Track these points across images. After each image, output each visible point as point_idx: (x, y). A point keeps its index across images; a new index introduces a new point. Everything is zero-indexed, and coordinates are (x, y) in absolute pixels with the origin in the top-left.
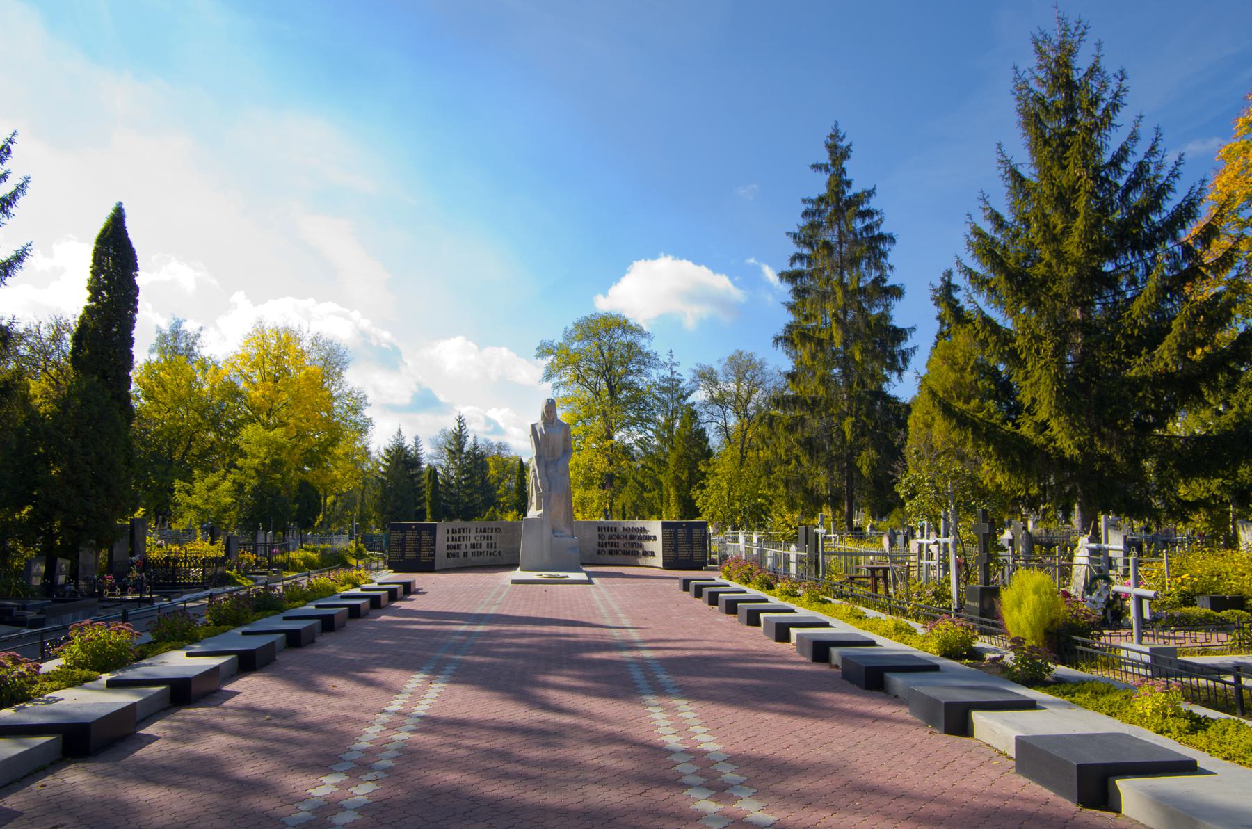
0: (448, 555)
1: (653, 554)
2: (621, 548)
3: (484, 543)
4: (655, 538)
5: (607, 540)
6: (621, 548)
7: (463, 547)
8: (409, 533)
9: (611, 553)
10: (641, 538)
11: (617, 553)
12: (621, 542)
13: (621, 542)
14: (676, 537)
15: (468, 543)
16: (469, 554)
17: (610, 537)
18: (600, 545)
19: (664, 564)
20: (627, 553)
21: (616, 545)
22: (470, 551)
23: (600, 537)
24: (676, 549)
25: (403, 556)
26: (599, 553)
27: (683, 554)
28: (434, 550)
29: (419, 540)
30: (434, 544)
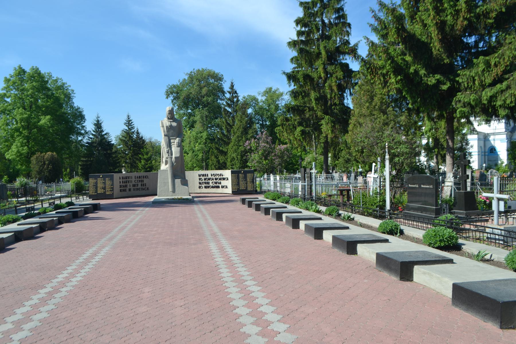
0: (121, 191)
2: (211, 184)
3: (140, 184)
5: (203, 181)
6: (211, 184)
7: (128, 186)
9: (206, 187)
11: (208, 187)
12: (211, 182)
13: (211, 182)
14: (238, 178)
15: (131, 184)
16: (132, 190)
17: (205, 179)
18: (200, 183)
19: (232, 191)
20: (213, 187)
21: (208, 183)
22: (132, 188)
23: (200, 179)
24: (238, 184)
25: (96, 191)
26: (200, 187)
27: (242, 187)
28: (113, 188)
29: (105, 183)
30: (113, 185)
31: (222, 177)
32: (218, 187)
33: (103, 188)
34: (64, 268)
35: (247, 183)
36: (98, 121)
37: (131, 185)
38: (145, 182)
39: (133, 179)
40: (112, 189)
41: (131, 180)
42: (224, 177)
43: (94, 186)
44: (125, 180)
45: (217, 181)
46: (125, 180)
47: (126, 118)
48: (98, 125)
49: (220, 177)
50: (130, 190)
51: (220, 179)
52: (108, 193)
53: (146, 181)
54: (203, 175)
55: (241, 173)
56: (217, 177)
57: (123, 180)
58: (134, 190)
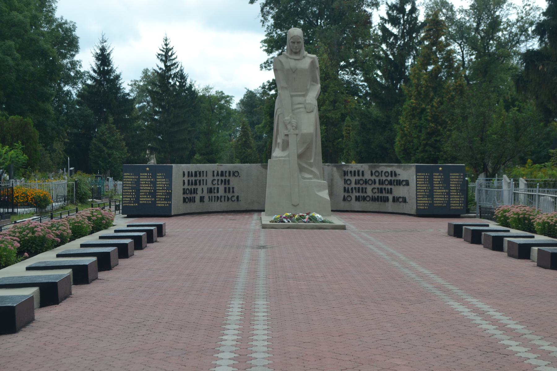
0: (184, 200)
1: (405, 200)
2: (369, 193)
3: (222, 188)
4: (407, 183)
5: (353, 185)
6: (369, 193)
7: (199, 191)
8: (143, 176)
9: (358, 199)
11: (364, 199)
12: (369, 188)
16: (206, 199)
20: (374, 199)
21: (364, 190)
23: (346, 181)
24: (431, 195)
25: (137, 200)
26: (344, 199)
28: (170, 194)
29: (154, 183)
30: (170, 187)
31: (394, 178)
32: (386, 200)
33: (150, 193)
34: (218, 326)
35: (448, 194)
36: (103, 49)
37: (205, 191)
38: (231, 185)
39: (210, 178)
40: (169, 196)
41: (205, 178)
42: (398, 178)
43: (132, 188)
44: (193, 179)
45: (384, 186)
46: (193, 179)
47: (161, 45)
48: (103, 58)
49: (389, 178)
50: (202, 199)
51: (390, 183)
52: (160, 204)
53: (234, 182)
54: (354, 173)
55: (438, 171)
56: (384, 178)
57: (190, 179)
58: (210, 199)
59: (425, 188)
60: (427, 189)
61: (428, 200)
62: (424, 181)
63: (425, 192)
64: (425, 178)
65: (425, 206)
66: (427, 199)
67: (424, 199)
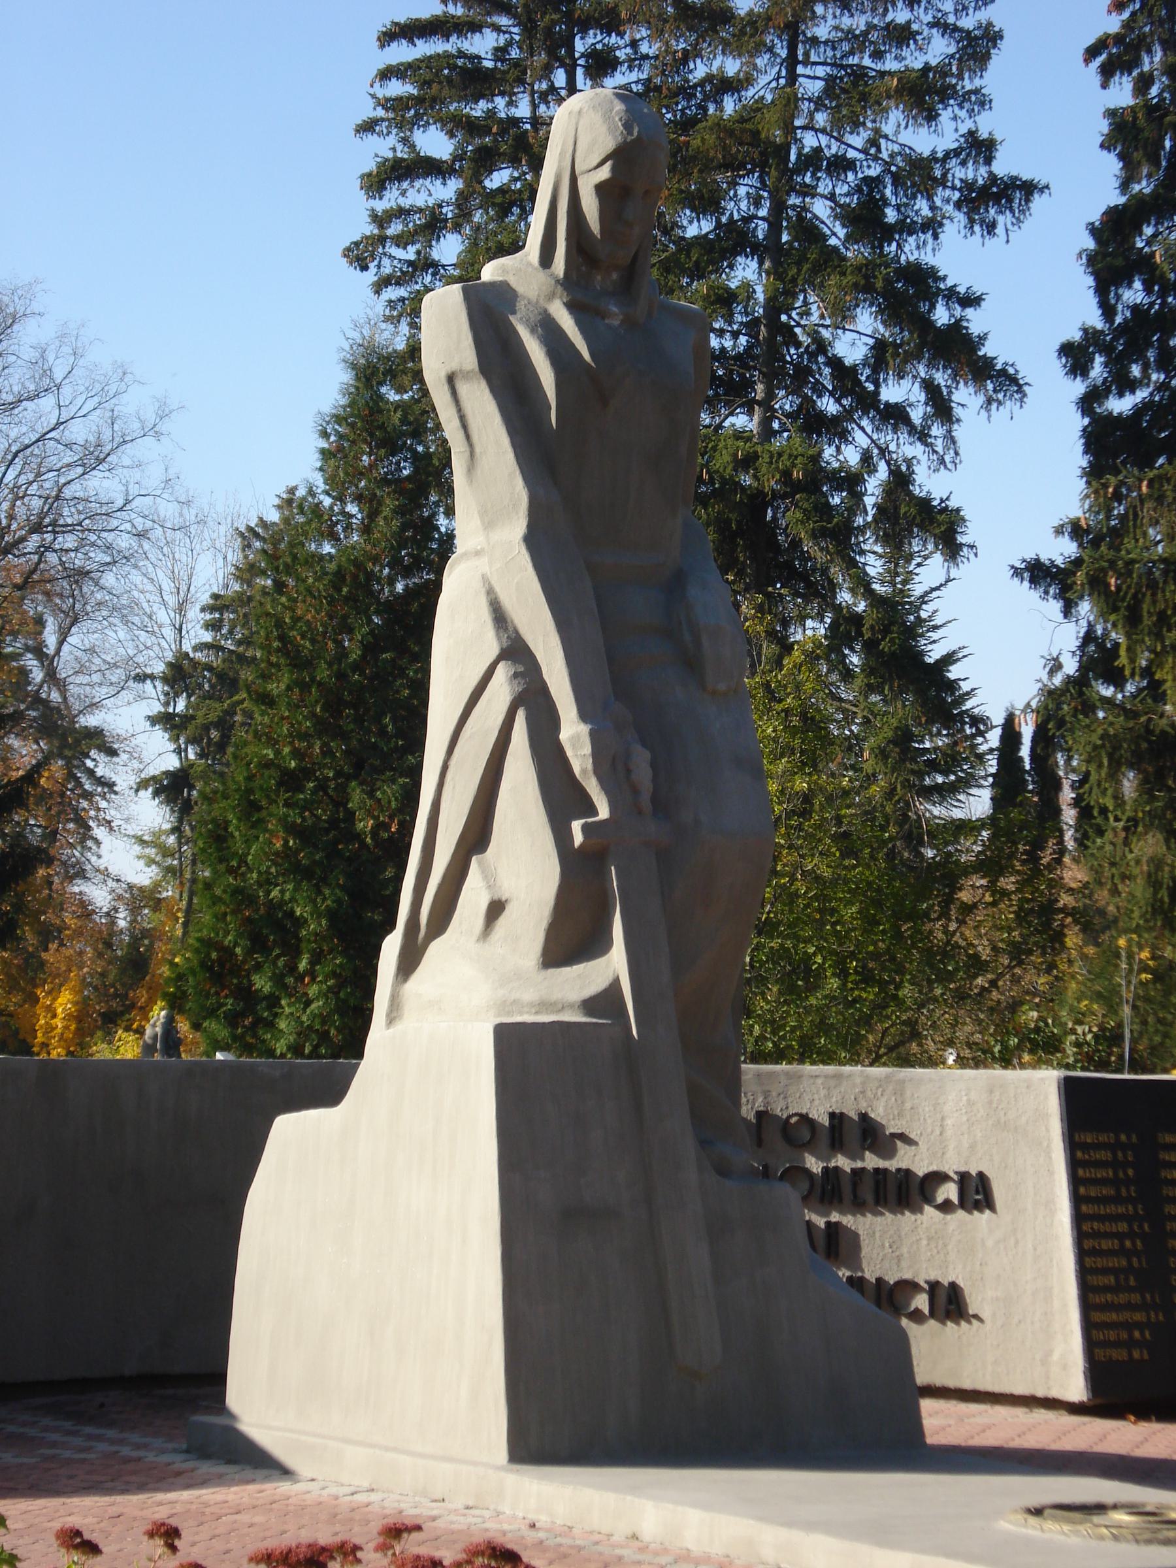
1: (950, 1304)
4: (977, 1193)
10: (830, 1190)
59: (1123, 1227)
60: (1131, 1235)
61: (1143, 1307)
62: (1115, 1182)
63: (1122, 1252)
64: (1114, 1164)
65: (1130, 1344)
66: (1136, 1298)
67: (1122, 1298)
